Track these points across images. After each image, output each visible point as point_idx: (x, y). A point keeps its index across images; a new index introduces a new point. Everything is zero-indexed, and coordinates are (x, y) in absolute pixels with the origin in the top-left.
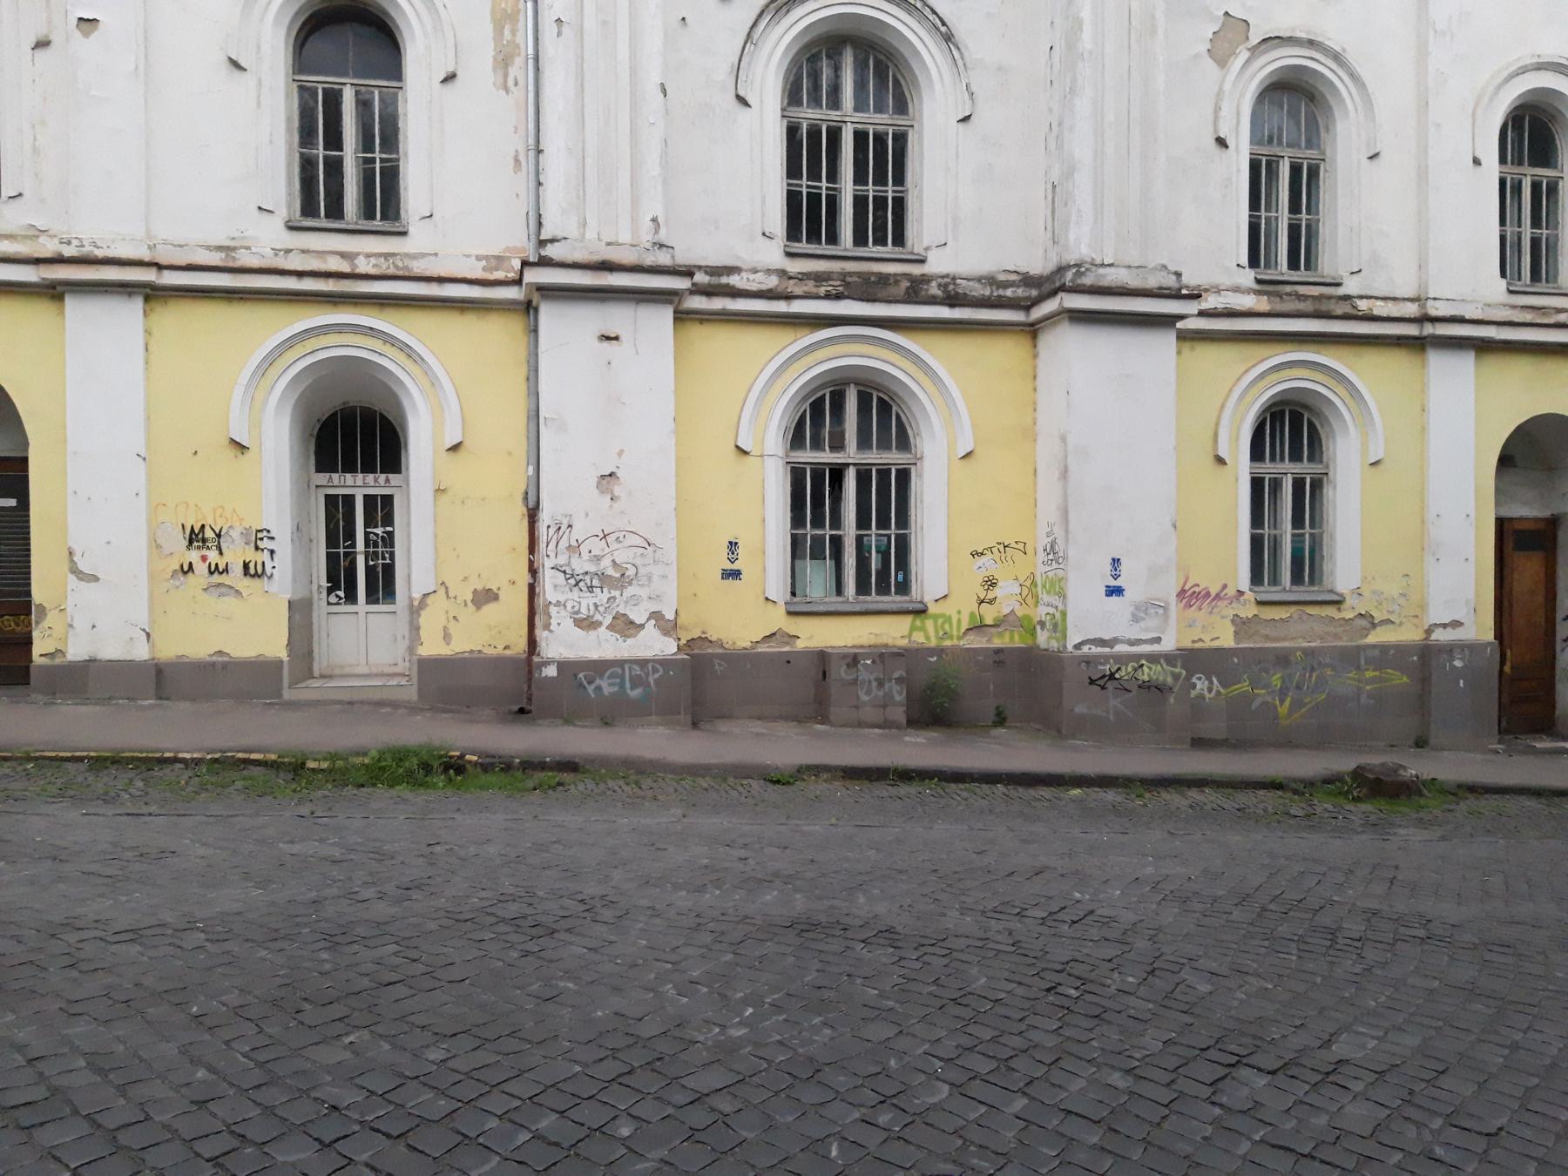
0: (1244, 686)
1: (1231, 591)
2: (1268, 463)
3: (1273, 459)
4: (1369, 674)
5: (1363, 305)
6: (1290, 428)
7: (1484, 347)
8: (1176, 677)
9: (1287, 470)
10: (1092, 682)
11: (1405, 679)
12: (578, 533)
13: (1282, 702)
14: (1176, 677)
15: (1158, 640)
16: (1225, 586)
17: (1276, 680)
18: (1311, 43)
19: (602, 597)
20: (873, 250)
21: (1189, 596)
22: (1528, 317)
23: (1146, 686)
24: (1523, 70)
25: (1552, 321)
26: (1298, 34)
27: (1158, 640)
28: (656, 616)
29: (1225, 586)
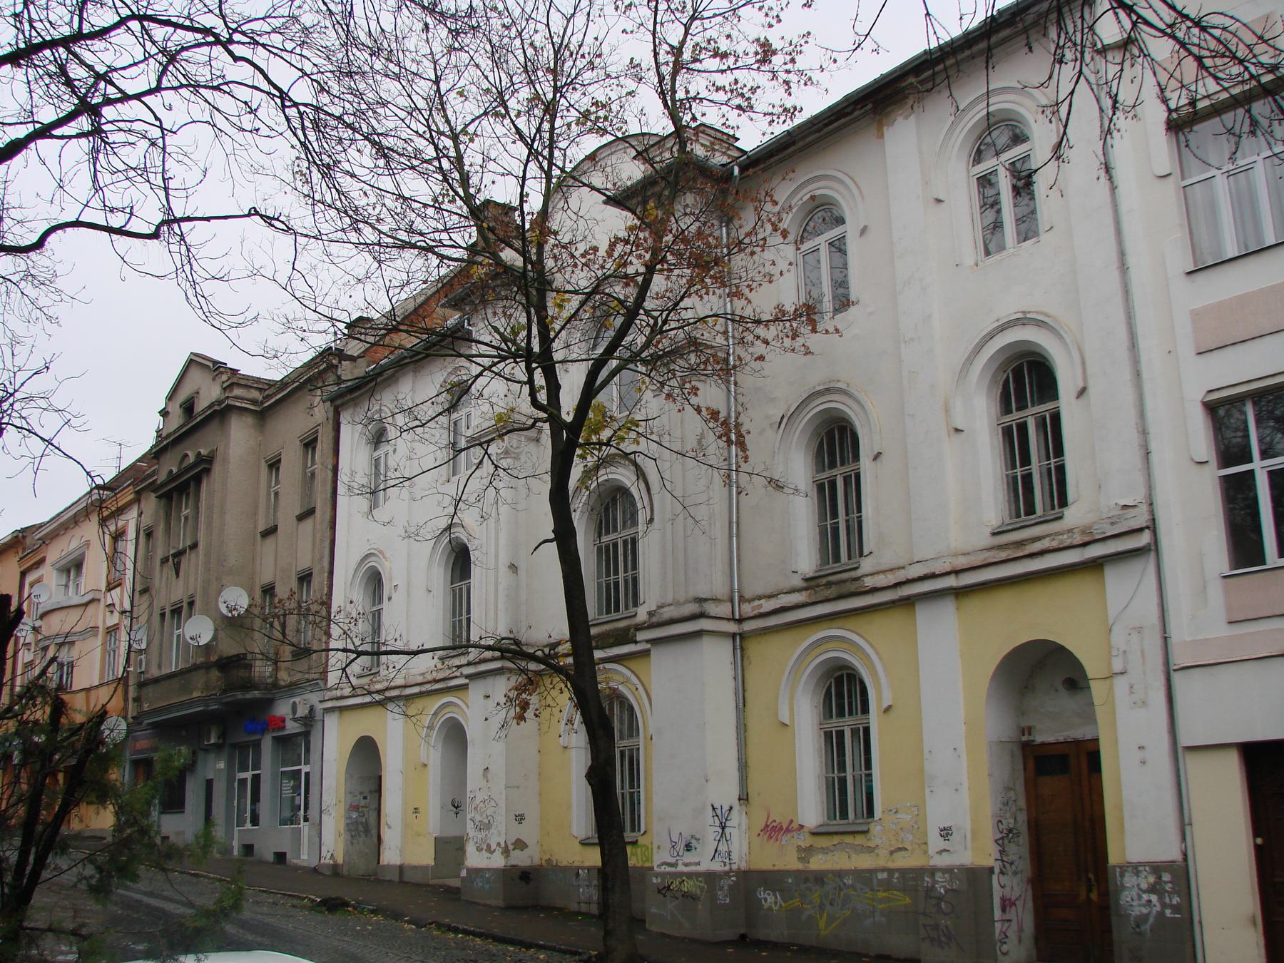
0: (796, 902)
1: (795, 825)
2: (834, 720)
3: (851, 714)
4: (881, 895)
5: (869, 582)
6: (843, 690)
7: (960, 593)
8: (702, 889)
9: (846, 724)
10: (659, 891)
11: (908, 900)
12: (477, 801)
13: (821, 916)
14: (702, 889)
15: (698, 864)
16: (792, 821)
17: (816, 897)
18: (829, 391)
19: (484, 834)
20: (614, 616)
21: (773, 830)
22: (1003, 555)
23: (686, 895)
24: (991, 336)
25: (1026, 552)
26: (819, 388)
27: (698, 864)
28: (499, 844)
29: (792, 821)
